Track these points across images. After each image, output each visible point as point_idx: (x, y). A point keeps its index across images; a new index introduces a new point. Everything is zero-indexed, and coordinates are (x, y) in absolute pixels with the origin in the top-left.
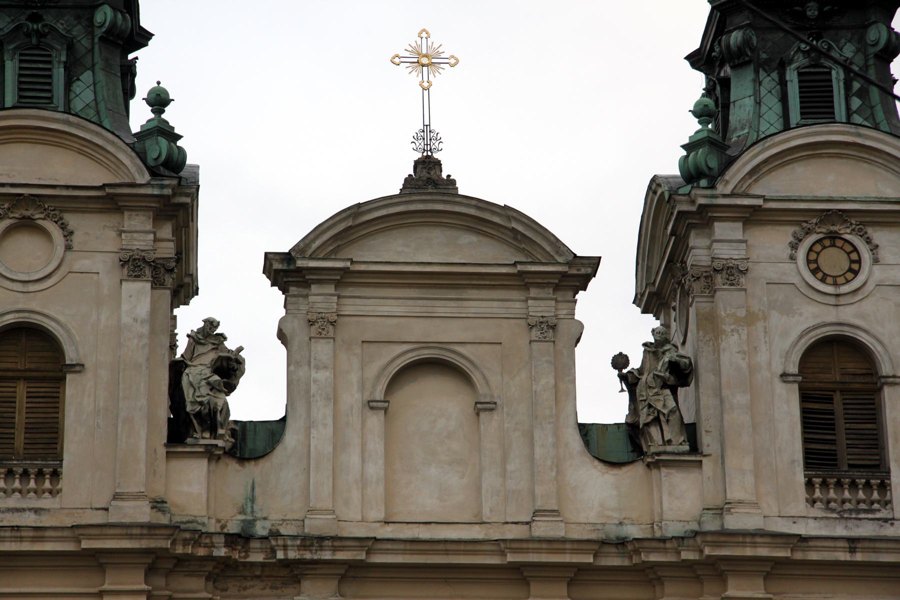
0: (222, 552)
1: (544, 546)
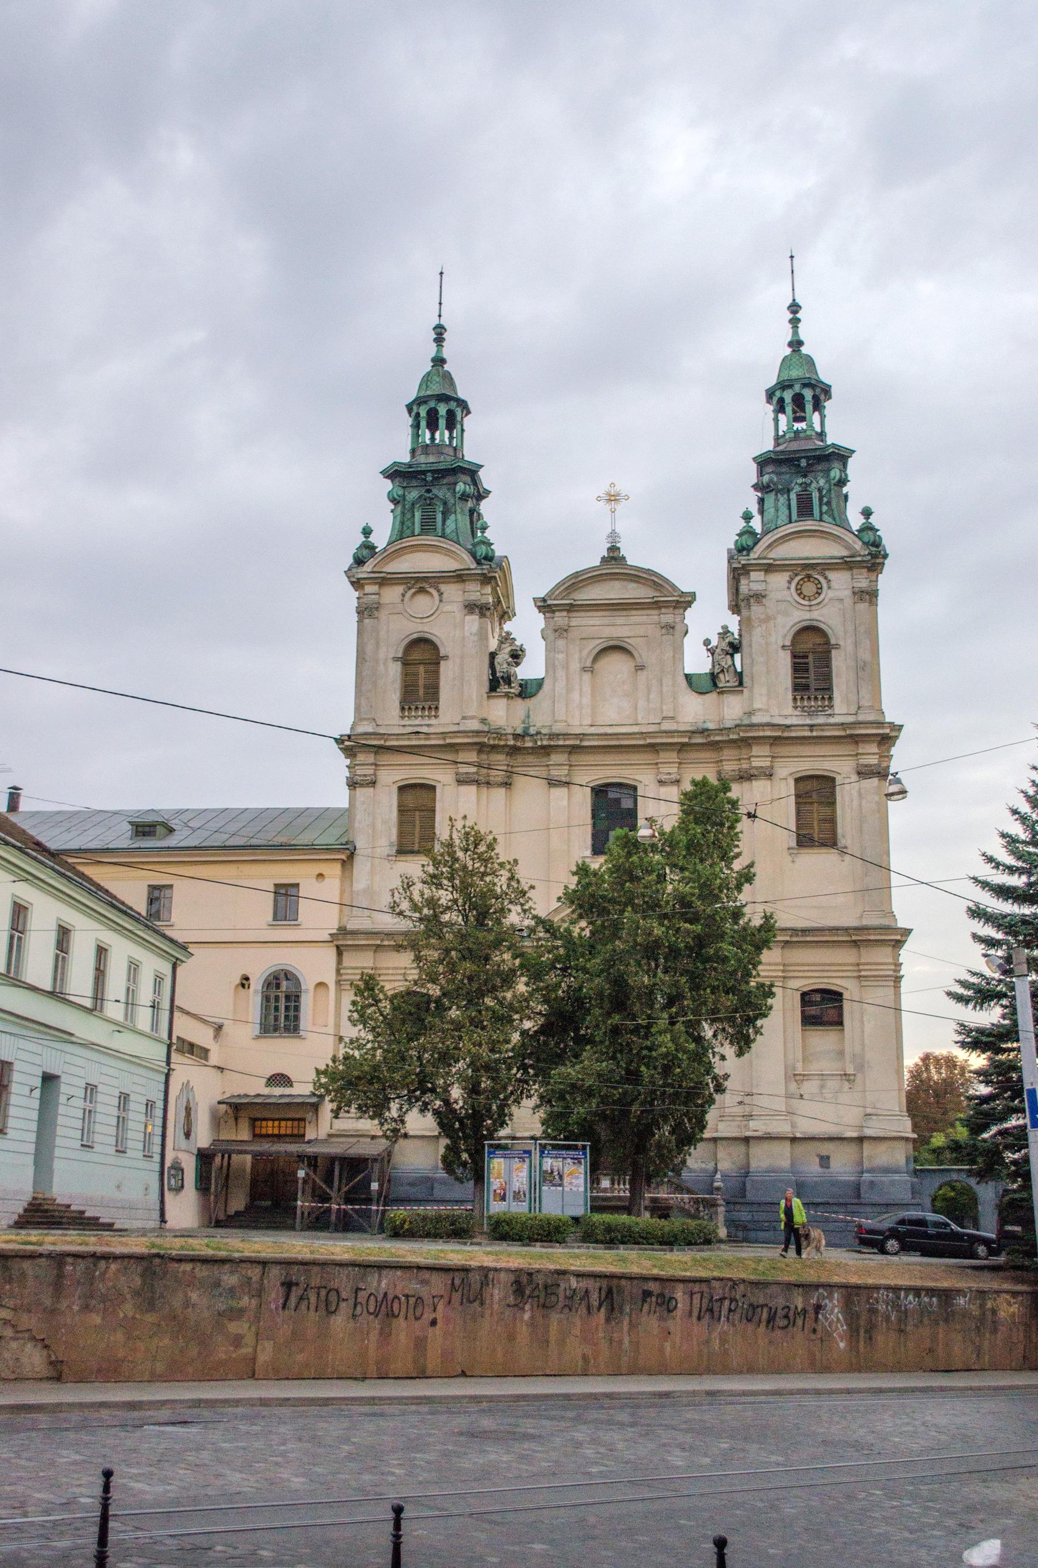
0: (511, 743)
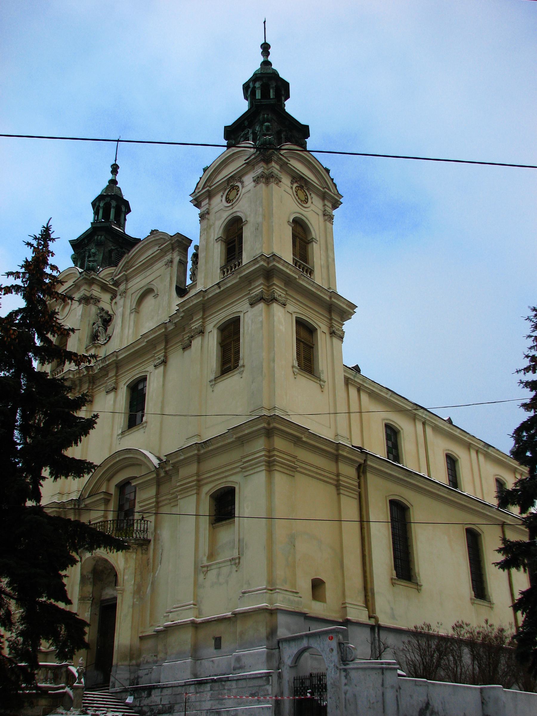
0: (85, 373)
1: (151, 332)
